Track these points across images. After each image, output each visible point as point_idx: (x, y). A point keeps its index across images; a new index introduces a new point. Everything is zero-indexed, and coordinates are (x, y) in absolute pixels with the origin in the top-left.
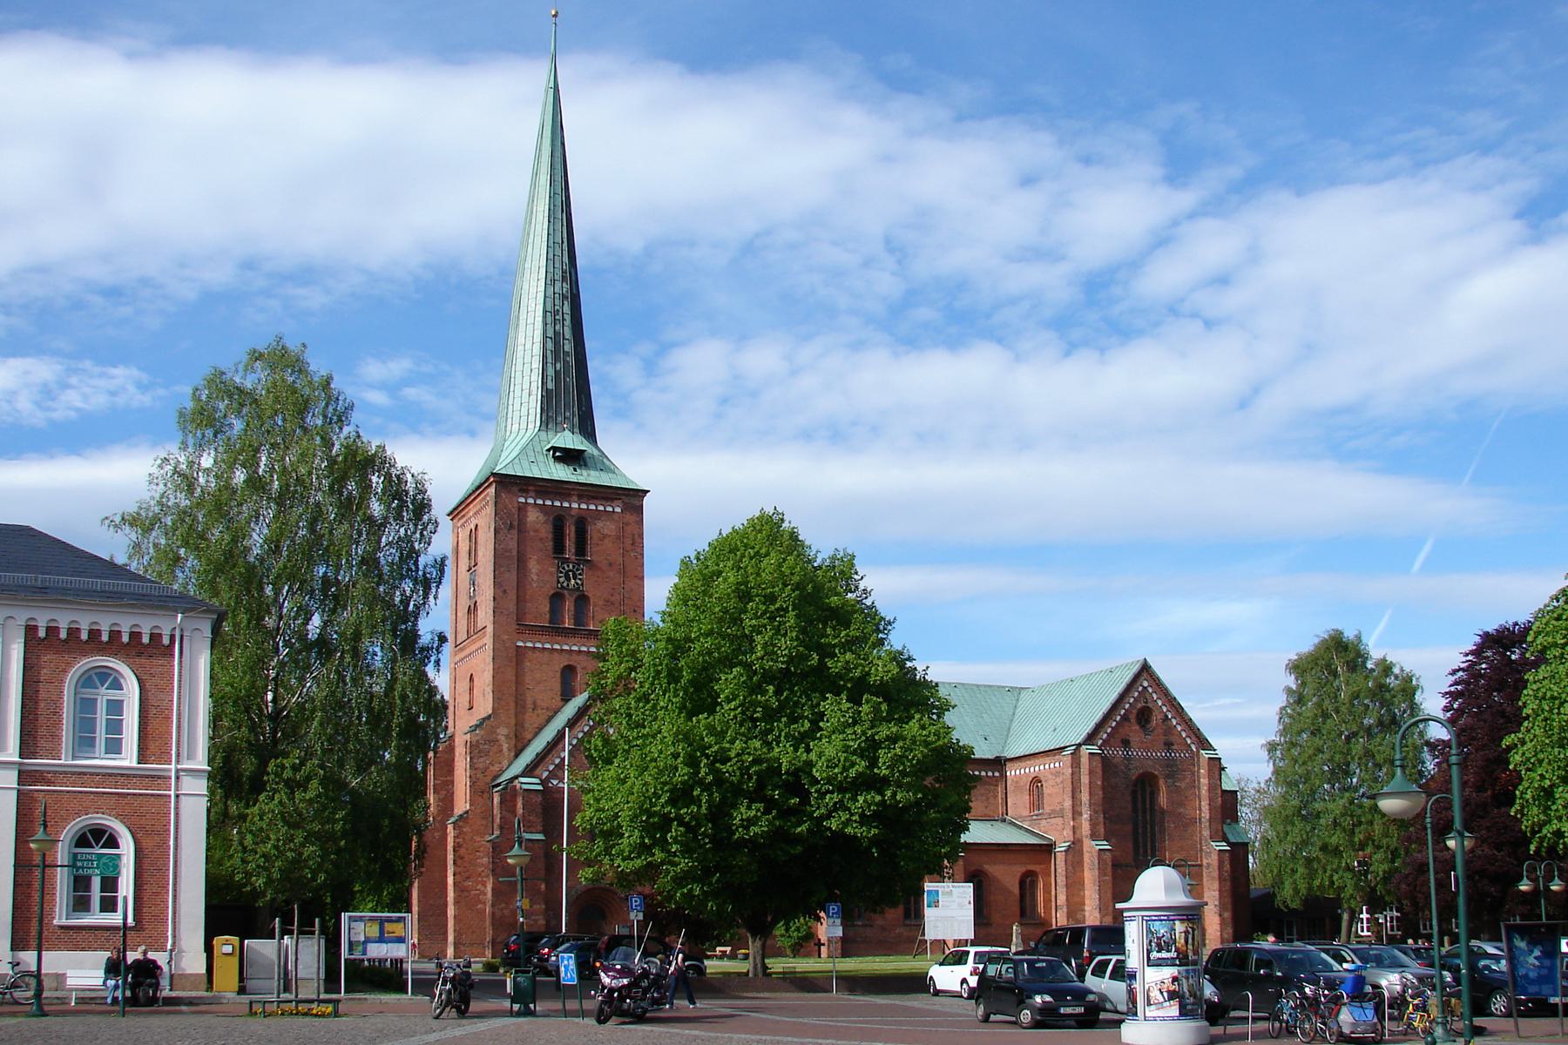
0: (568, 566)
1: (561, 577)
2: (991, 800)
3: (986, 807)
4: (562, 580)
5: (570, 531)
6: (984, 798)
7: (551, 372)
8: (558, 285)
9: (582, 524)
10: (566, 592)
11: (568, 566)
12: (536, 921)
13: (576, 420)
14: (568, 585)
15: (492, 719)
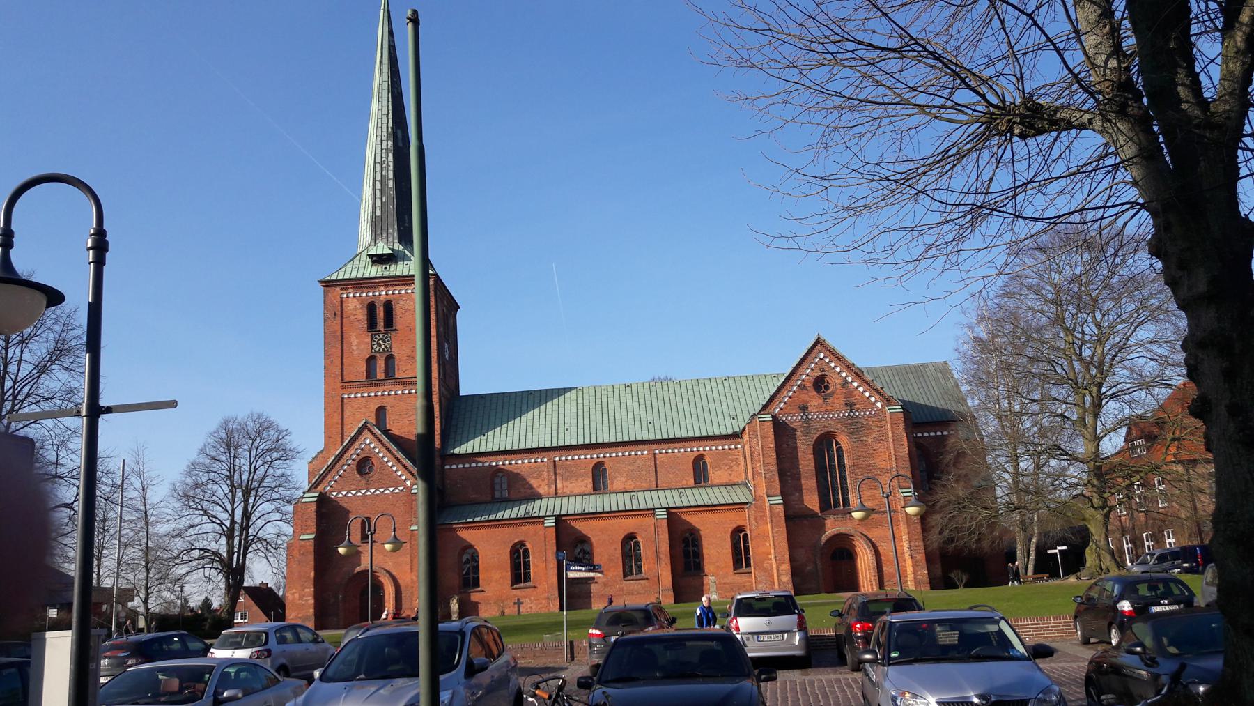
3: (730, 475)
4: (374, 347)
5: (381, 313)
7: (378, 204)
8: (384, 144)
9: (388, 306)
10: (377, 355)
13: (396, 234)
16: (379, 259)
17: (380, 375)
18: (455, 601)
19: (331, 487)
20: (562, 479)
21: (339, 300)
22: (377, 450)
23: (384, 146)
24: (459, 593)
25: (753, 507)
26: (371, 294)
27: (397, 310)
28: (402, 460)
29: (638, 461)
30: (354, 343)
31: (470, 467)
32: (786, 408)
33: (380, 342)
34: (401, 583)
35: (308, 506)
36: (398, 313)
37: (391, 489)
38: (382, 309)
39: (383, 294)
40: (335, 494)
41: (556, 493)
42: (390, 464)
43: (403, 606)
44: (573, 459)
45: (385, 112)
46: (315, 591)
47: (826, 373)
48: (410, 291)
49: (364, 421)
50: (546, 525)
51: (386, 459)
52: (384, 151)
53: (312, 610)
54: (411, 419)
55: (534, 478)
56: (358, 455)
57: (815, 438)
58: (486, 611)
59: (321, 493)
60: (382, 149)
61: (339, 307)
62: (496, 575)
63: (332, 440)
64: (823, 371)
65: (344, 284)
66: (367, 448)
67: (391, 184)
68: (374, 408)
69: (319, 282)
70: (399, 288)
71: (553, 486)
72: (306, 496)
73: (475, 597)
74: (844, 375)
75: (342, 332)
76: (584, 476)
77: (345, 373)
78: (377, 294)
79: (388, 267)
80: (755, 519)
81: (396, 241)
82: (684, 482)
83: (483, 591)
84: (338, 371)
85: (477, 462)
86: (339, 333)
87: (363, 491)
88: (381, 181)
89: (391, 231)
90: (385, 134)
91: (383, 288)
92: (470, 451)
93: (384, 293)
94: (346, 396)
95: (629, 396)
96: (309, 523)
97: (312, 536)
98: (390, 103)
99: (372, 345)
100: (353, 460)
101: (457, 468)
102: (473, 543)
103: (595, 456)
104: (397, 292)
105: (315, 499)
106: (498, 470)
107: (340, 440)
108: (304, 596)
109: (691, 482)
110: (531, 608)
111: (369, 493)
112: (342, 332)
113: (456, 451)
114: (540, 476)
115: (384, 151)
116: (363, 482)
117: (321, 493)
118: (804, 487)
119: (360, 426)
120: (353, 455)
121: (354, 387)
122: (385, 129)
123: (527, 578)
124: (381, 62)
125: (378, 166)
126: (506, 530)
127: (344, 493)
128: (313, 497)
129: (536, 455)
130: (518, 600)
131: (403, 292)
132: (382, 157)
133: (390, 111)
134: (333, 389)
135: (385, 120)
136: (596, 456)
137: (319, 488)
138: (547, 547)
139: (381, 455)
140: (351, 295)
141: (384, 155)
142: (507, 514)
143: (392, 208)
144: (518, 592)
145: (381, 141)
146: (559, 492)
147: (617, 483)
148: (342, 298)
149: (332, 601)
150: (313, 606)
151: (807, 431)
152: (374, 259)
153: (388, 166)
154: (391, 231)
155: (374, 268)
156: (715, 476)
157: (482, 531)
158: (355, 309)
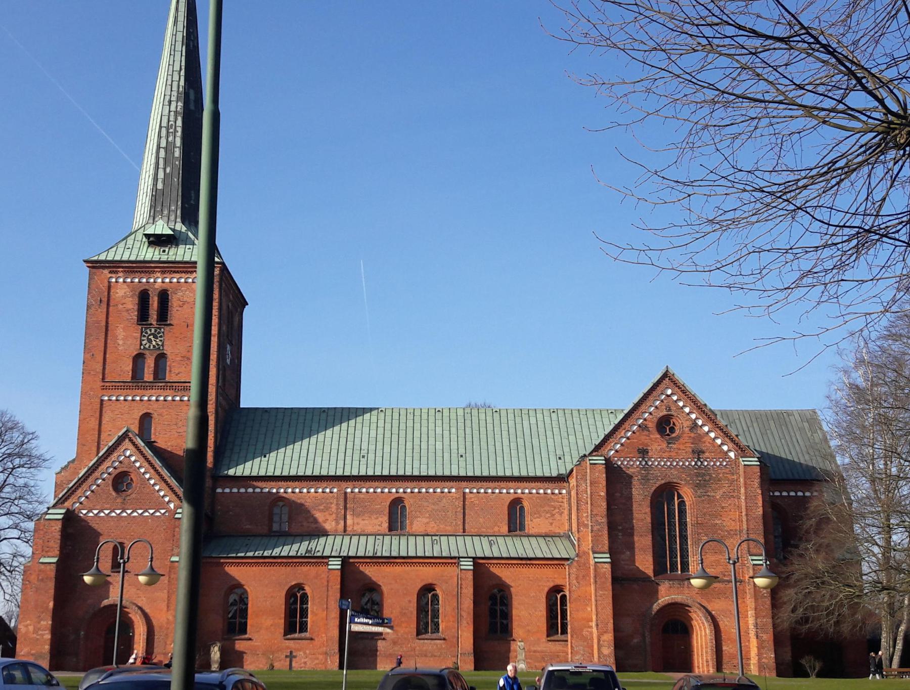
0: (151, 331)
1: (144, 340)
2: (557, 516)
3: (551, 524)
4: (144, 342)
5: (154, 303)
6: (549, 515)
7: (161, 175)
8: (173, 105)
9: (164, 296)
11: (151, 331)
12: (42, 635)
13: (179, 212)
14: (149, 347)
15: (76, 463)
16: (157, 240)
17: (148, 376)
18: (216, 649)
19: (81, 503)
20: (353, 515)
21: (106, 284)
22: (138, 464)
23: (173, 108)
24: (223, 640)
25: (575, 564)
26: (144, 280)
27: (174, 302)
28: (166, 478)
29: (444, 500)
30: (120, 337)
31: (246, 492)
32: (622, 451)
33: (152, 337)
34: (155, 622)
35: (53, 523)
36: (175, 304)
37: (151, 511)
38: (156, 299)
39: (158, 281)
40: (84, 512)
41: (345, 531)
42: (152, 482)
43: (155, 650)
44: (367, 492)
45: (177, 67)
46: (52, 625)
47: (672, 413)
48: (190, 280)
49: (125, 429)
50: (330, 567)
51: (147, 476)
52: (172, 113)
53: (47, 647)
54: (180, 430)
55: (322, 511)
56: (115, 468)
57: (653, 489)
58: (251, 664)
59: (68, 510)
60: (170, 111)
61: (106, 294)
62: (267, 621)
63: (85, 448)
64: (670, 410)
65: (114, 266)
66: (126, 461)
67: (177, 153)
68: (137, 414)
69: (85, 261)
70: (178, 275)
71: (342, 523)
72: (50, 511)
73: (240, 645)
74: (693, 416)
75: (107, 323)
76: (379, 512)
77: (107, 372)
78: (152, 280)
79: (167, 250)
80: (577, 578)
81: (179, 220)
82: (496, 529)
83: (250, 639)
84: (99, 368)
85: (254, 487)
86: (104, 323)
87: (118, 512)
88: (166, 149)
89: (173, 208)
90: (175, 93)
91: (159, 275)
92: (247, 473)
93: (160, 280)
94: (106, 398)
95: (439, 423)
96: (52, 544)
97: (55, 560)
98: (183, 58)
99: (141, 341)
100: (109, 474)
101: (231, 492)
102: (243, 582)
103: (394, 490)
104: (175, 280)
105: (60, 517)
106: (278, 498)
107: (95, 449)
108: (39, 629)
109: (505, 529)
110: (305, 663)
111: (124, 514)
112: (107, 323)
113: (231, 472)
114: (327, 509)
115: (172, 113)
116: (119, 500)
117: (68, 510)
118: (637, 545)
119: (120, 434)
120: (109, 468)
121: (116, 388)
122: (175, 88)
123: (303, 628)
124: (177, 9)
125: (164, 131)
126: (284, 570)
127: (96, 512)
128: (58, 514)
129: (325, 484)
130: (291, 652)
131: (183, 280)
132: (169, 121)
133: (183, 67)
134: (91, 389)
135: (176, 77)
136: (396, 490)
137: (66, 504)
138: (330, 593)
139: (142, 470)
140: (121, 280)
141: (172, 118)
142: (285, 551)
143: (177, 181)
144: (291, 644)
145: (170, 102)
146: (349, 529)
147: (417, 524)
148: (109, 282)
149: (72, 637)
150: (49, 642)
151: (645, 479)
152: (151, 239)
153: (176, 131)
154: (173, 208)
155: (151, 250)
156: (533, 524)
157: (254, 568)
158: (124, 297)
